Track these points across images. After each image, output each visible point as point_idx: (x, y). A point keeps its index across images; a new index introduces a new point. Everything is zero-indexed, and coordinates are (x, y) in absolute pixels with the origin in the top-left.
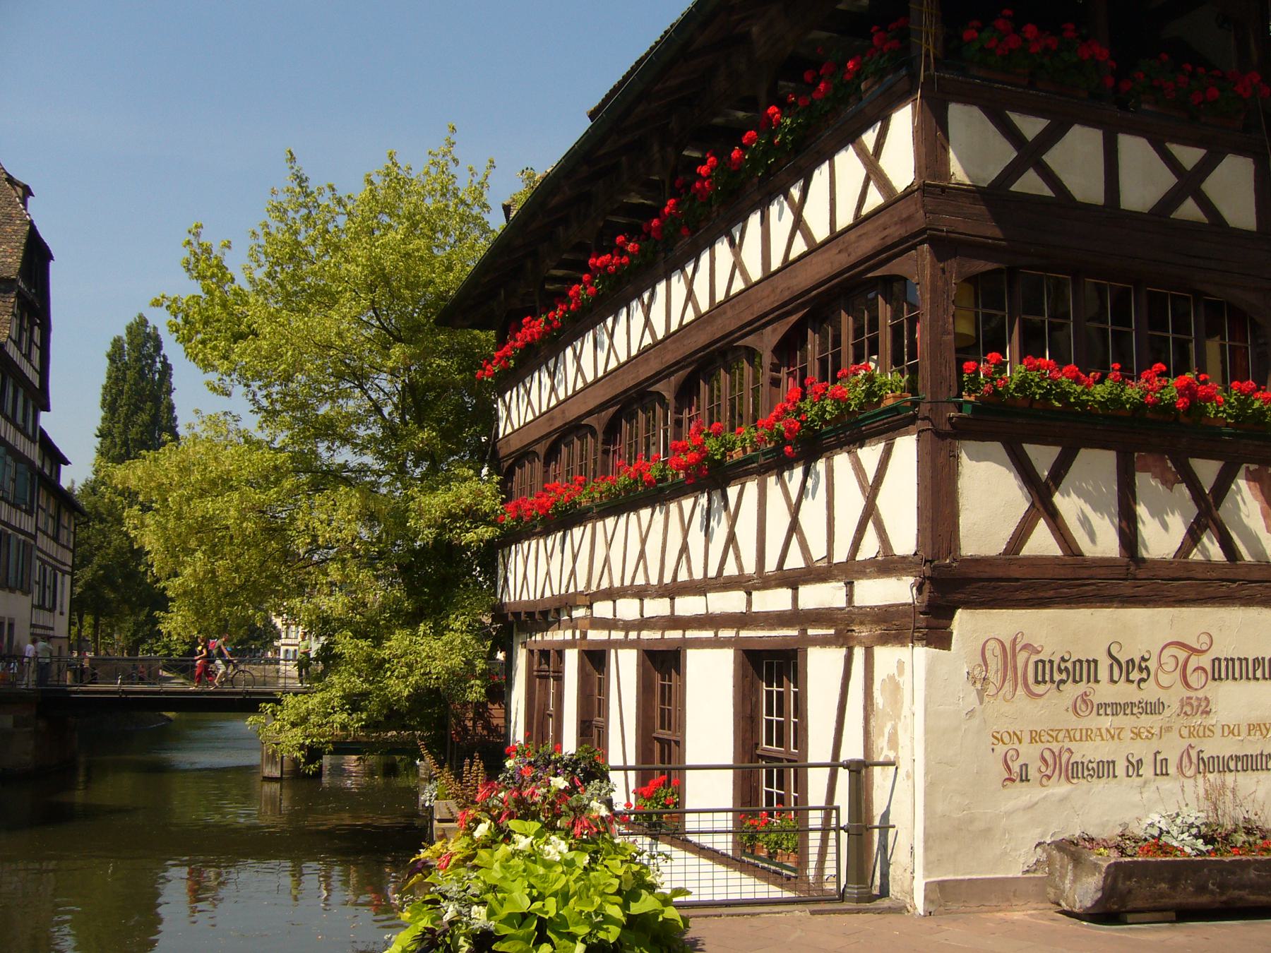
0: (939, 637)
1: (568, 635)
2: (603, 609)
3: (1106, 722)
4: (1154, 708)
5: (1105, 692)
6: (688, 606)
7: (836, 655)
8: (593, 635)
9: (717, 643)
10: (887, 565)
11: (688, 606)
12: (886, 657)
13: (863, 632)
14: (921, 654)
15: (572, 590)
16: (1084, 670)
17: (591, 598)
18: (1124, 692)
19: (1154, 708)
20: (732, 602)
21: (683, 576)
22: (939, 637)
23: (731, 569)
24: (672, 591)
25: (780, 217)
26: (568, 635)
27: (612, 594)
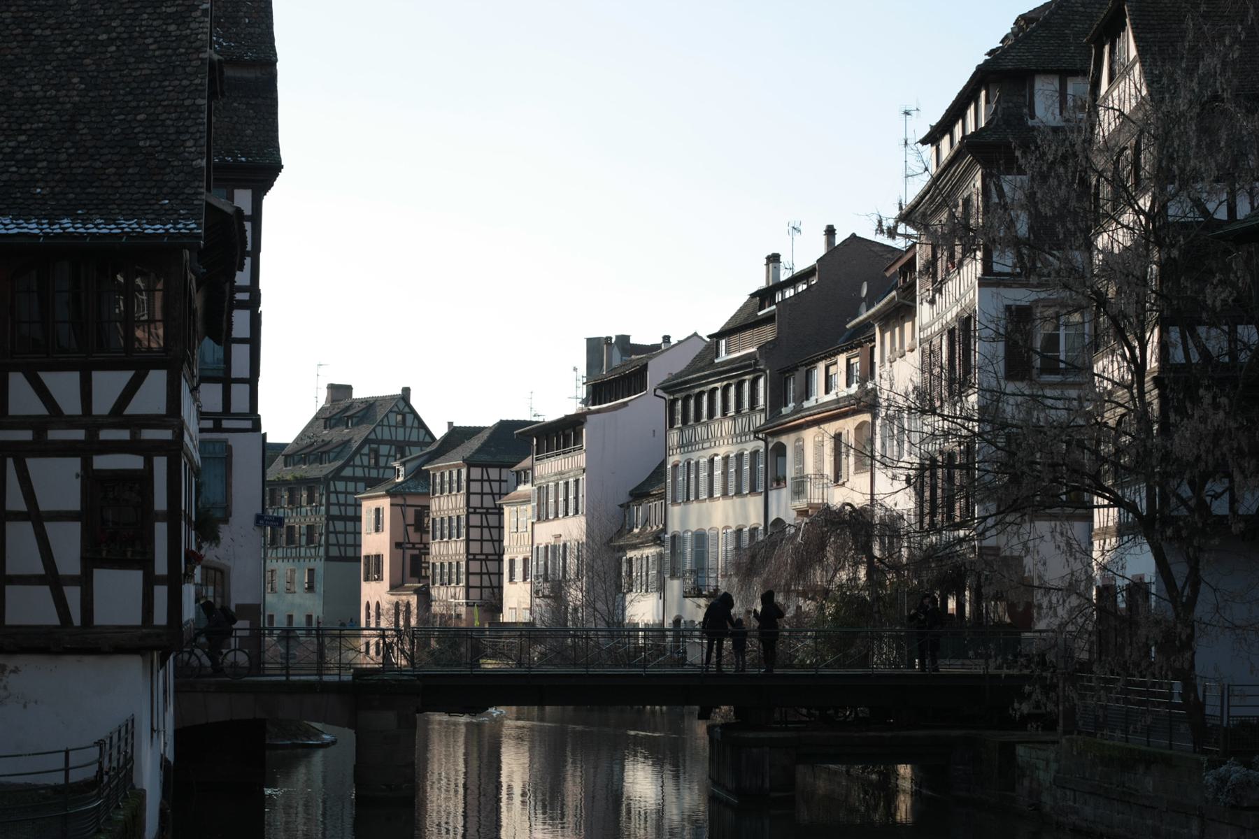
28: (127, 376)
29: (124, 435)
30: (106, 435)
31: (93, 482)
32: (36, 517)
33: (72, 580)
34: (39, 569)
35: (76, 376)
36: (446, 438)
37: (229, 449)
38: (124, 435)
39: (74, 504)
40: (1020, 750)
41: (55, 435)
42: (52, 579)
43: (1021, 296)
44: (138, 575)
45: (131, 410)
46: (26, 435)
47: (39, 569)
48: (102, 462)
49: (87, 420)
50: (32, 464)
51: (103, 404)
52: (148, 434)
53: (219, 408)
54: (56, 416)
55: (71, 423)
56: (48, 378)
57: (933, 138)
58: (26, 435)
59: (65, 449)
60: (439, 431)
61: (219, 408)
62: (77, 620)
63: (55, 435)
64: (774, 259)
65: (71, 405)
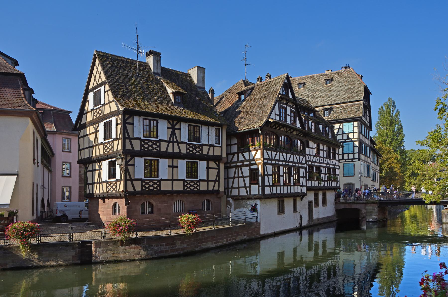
31: (251, 171)
32: (243, 177)
34: (244, 186)
37: (354, 164)
39: (248, 175)
42: (245, 187)
44: (257, 186)
46: (241, 164)
47: (244, 186)
48: (252, 167)
50: (242, 168)
53: (353, 158)
54: (246, 160)
55: (247, 161)
58: (241, 164)
59: (247, 165)
61: (353, 158)
62: (249, 194)
63: (245, 163)
65: (247, 158)
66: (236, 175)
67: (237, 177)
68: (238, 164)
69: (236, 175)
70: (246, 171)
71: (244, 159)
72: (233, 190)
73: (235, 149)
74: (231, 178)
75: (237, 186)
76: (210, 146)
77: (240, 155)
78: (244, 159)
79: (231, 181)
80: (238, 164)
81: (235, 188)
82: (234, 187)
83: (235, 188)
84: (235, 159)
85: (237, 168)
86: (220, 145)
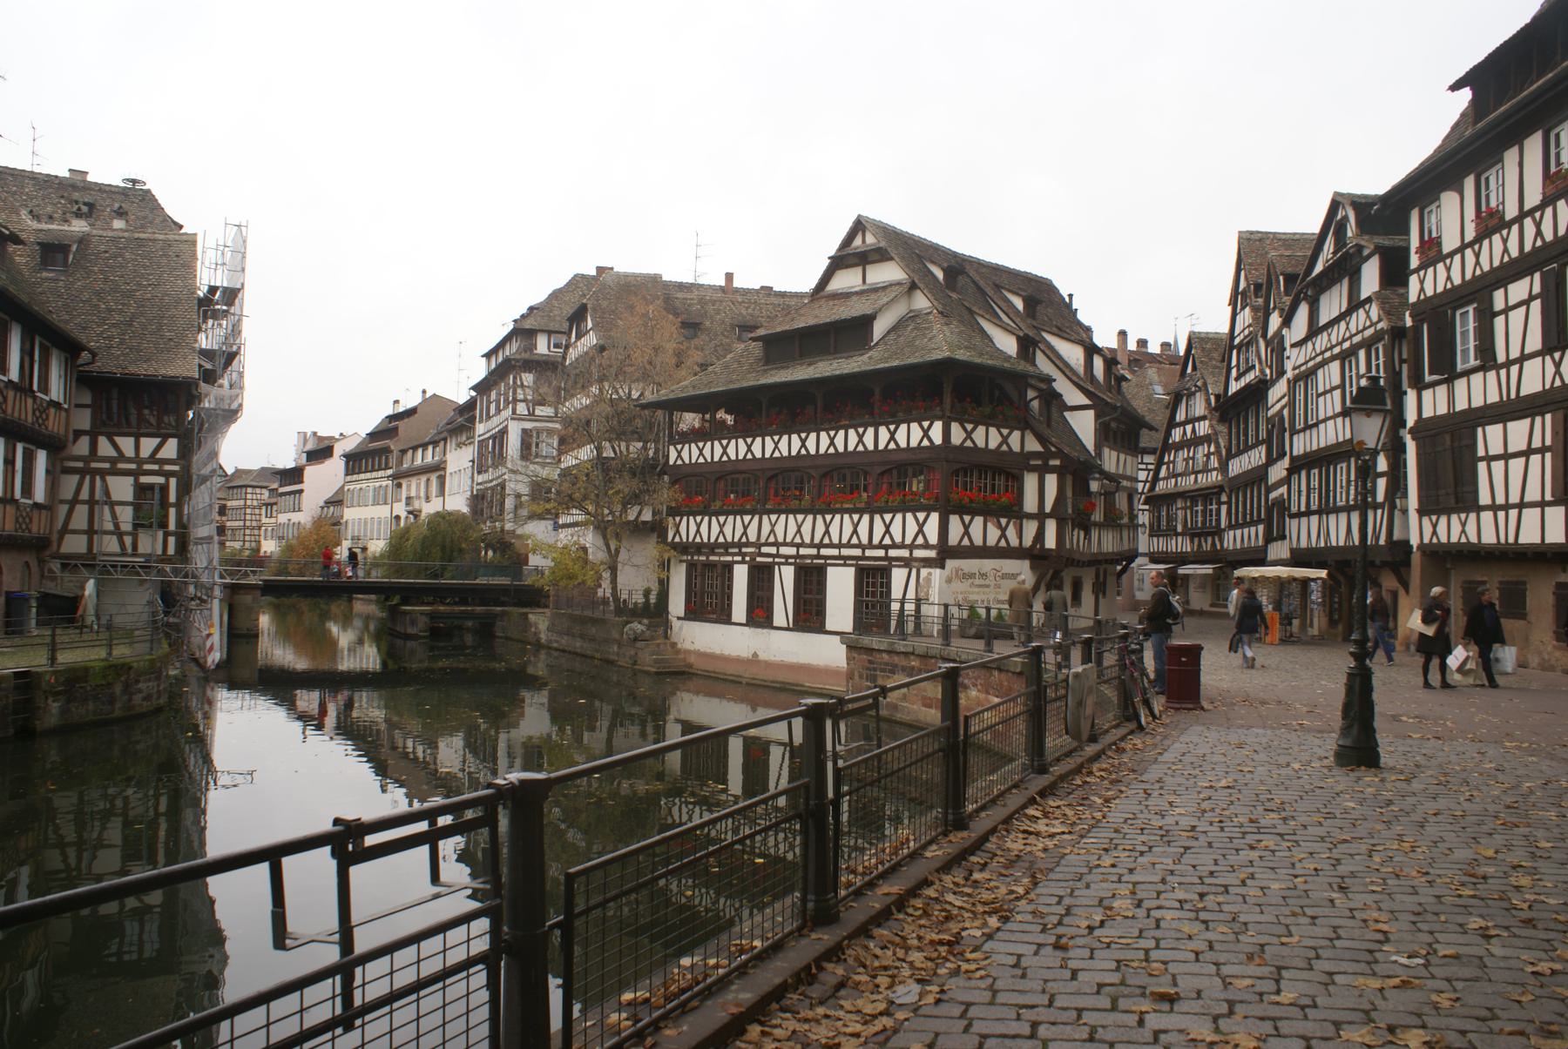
0: (943, 567)
1: (739, 558)
2: (773, 550)
3: (977, 590)
4: (988, 586)
5: (977, 582)
6: (824, 552)
7: (905, 571)
8: (758, 559)
9: (845, 565)
10: (926, 546)
11: (824, 552)
12: (924, 572)
13: (916, 564)
14: (938, 571)
15: (744, 540)
16: (972, 576)
17: (758, 545)
18: (981, 582)
19: (988, 586)
20: (857, 552)
21: (826, 541)
22: (943, 567)
23: (855, 541)
24: (820, 546)
25: (884, 433)
26: (739, 558)
27: (776, 544)
28: (158, 440)
29: (156, 467)
30: (146, 467)
32: (112, 504)
33: (128, 533)
35: (132, 440)
36: (233, 474)
38: (156, 467)
39: (130, 498)
40: (530, 616)
41: (121, 466)
43: (528, 425)
45: (159, 456)
46: (107, 465)
48: (144, 479)
49: (137, 459)
51: (145, 452)
52: (167, 467)
54: (121, 456)
55: (129, 460)
56: (118, 440)
57: (488, 356)
58: (107, 465)
60: (230, 471)
63: (121, 466)
64: (396, 402)
66: (84, 495)
67: (84, 502)
68: (94, 465)
69: (84, 495)
70: (122, 488)
71: (114, 454)
72: (68, 537)
73: (83, 420)
74: (62, 502)
75: (85, 526)
76: (57, 405)
77: (103, 442)
78: (114, 454)
79: (63, 510)
80: (94, 465)
81: (75, 532)
82: (72, 526)
83: (75, 532)
84: (82, 447)
85: (88, 478)
86: (66, 406)
